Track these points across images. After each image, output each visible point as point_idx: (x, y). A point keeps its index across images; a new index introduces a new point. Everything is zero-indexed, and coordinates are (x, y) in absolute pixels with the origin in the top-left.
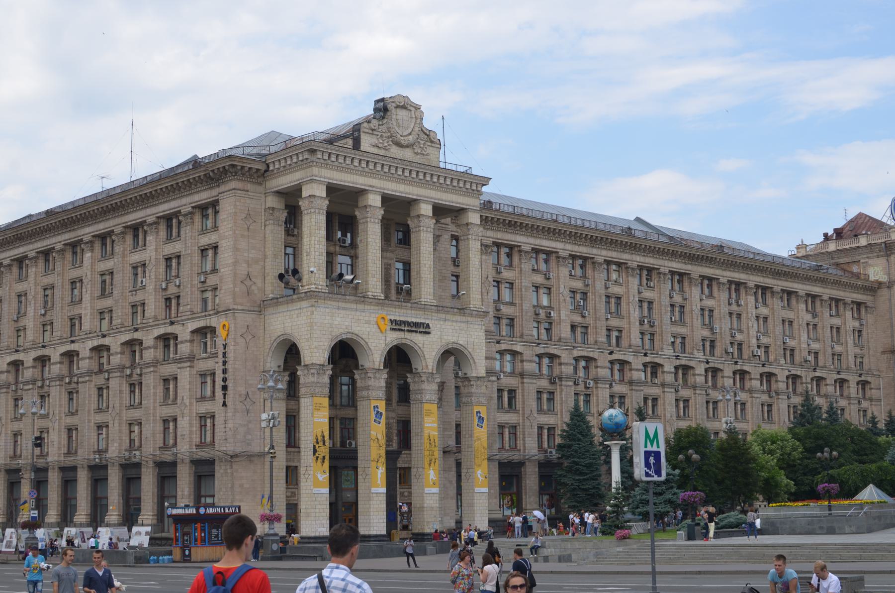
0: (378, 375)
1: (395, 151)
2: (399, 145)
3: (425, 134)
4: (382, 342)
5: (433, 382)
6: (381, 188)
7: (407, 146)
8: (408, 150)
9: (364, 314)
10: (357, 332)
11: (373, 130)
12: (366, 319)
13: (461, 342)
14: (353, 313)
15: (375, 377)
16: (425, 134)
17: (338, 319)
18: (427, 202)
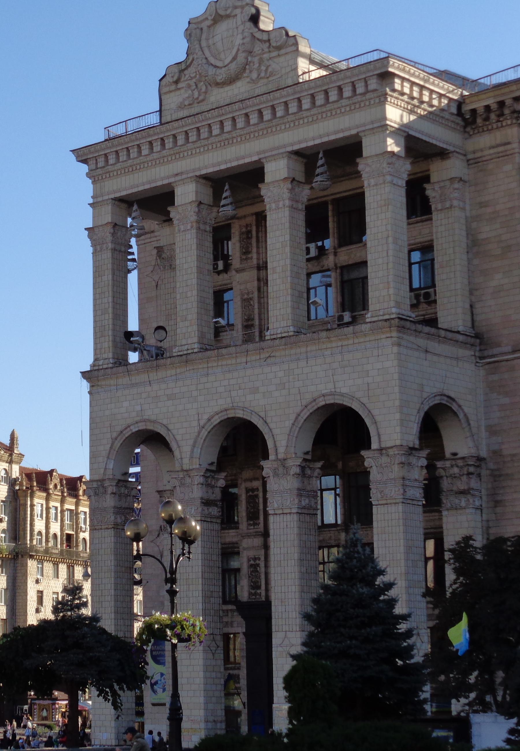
0: (188, 480)
1: (218, 96)
2: (218, 84)
3: (265, 41)
4: (195, 424)
5: (287, 473)
6: (194, 170)
7: (231, 81)
8: (239, 84)
9: (163, 386)
10: (153, 418)
11: (177, 82)
12: (169, 392)
13: (344, 390)
14: (148, 388)
15: (182, 485)
16: (265, 41)
17: (126, 404)
18: (274, 158)
